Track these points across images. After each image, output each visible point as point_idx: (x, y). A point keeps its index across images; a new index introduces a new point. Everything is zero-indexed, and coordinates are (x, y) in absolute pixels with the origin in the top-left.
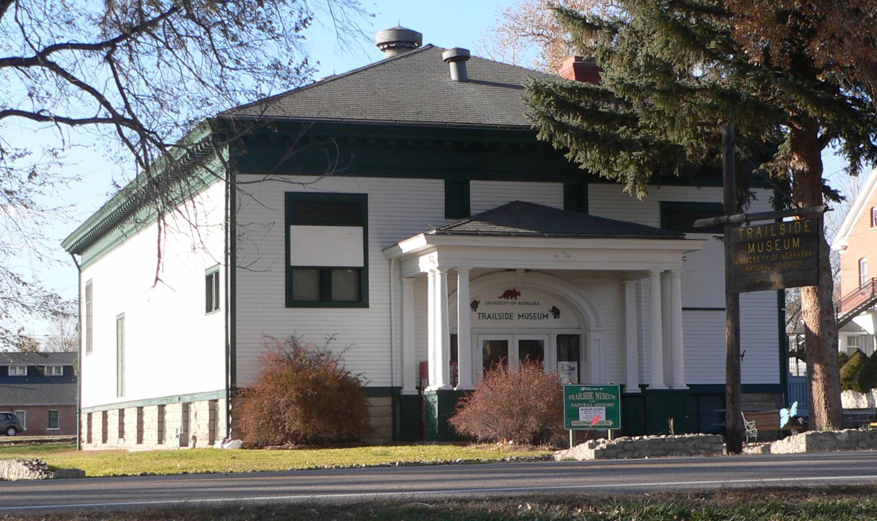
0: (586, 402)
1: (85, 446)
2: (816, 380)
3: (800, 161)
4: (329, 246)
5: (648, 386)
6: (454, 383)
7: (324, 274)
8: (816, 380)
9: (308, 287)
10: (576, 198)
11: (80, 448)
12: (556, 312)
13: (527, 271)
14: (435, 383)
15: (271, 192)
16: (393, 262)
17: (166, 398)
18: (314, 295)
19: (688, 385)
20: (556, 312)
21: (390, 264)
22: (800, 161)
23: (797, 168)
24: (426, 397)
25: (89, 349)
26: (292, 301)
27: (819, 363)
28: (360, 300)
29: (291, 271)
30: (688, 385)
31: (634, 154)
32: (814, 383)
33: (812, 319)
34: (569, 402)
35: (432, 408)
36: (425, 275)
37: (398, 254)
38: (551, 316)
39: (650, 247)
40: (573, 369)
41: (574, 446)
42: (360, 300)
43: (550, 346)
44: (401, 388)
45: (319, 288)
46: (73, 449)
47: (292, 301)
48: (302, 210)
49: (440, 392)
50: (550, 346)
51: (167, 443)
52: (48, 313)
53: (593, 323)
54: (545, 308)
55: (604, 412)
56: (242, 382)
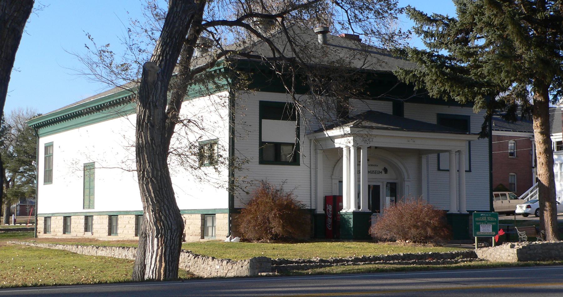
0: (483, 222)
1: (41, 235)
2: (546, 210)
3: (539, 96)
4: (280, 131)
5: (448, 211)
6: (359, 208)
7: (277, 146)
8: (546, 210)
9: (271, 154)
10: (398, 109)
11: (36, 236)
12: (386, 170)
13: (376, 148)
14: (349, 207)
15: (253, 99)
16: (312, 141)
17: (120, 212)
18: (272, 158)
19: (468, 211)
20: (386, 170)
21: (311, 143)
22: (539, 96)
23: (538, 99)
24: (342, 215)
25: (48, 179)
26: (262, 161)
27: (548, 201)
28: (295, 161)
29: (261, 143)
30: (468, 211)
31: (483, 89)
32: (545, 212)
33: (545, 178)
34: (475, 221)
35: (349, 222)
36: (341, 149)
37: (322, 137)
38: (383, 172)
39: (453, 138)
40: (393, 201)
41: (495, 246)
42: (295, 161)
43: (383, 188)
44: (315, 210)
45: (272, 154)
46: (31, 237)
47: (262, 161)
48: (269, 111)
49: (354, 213)
50: (383, 188)
51: (72, 233)
52: (189, 169)
53: (406, 177)
54: (380, 169)
55: (491, 227)
56: (237, 205)
